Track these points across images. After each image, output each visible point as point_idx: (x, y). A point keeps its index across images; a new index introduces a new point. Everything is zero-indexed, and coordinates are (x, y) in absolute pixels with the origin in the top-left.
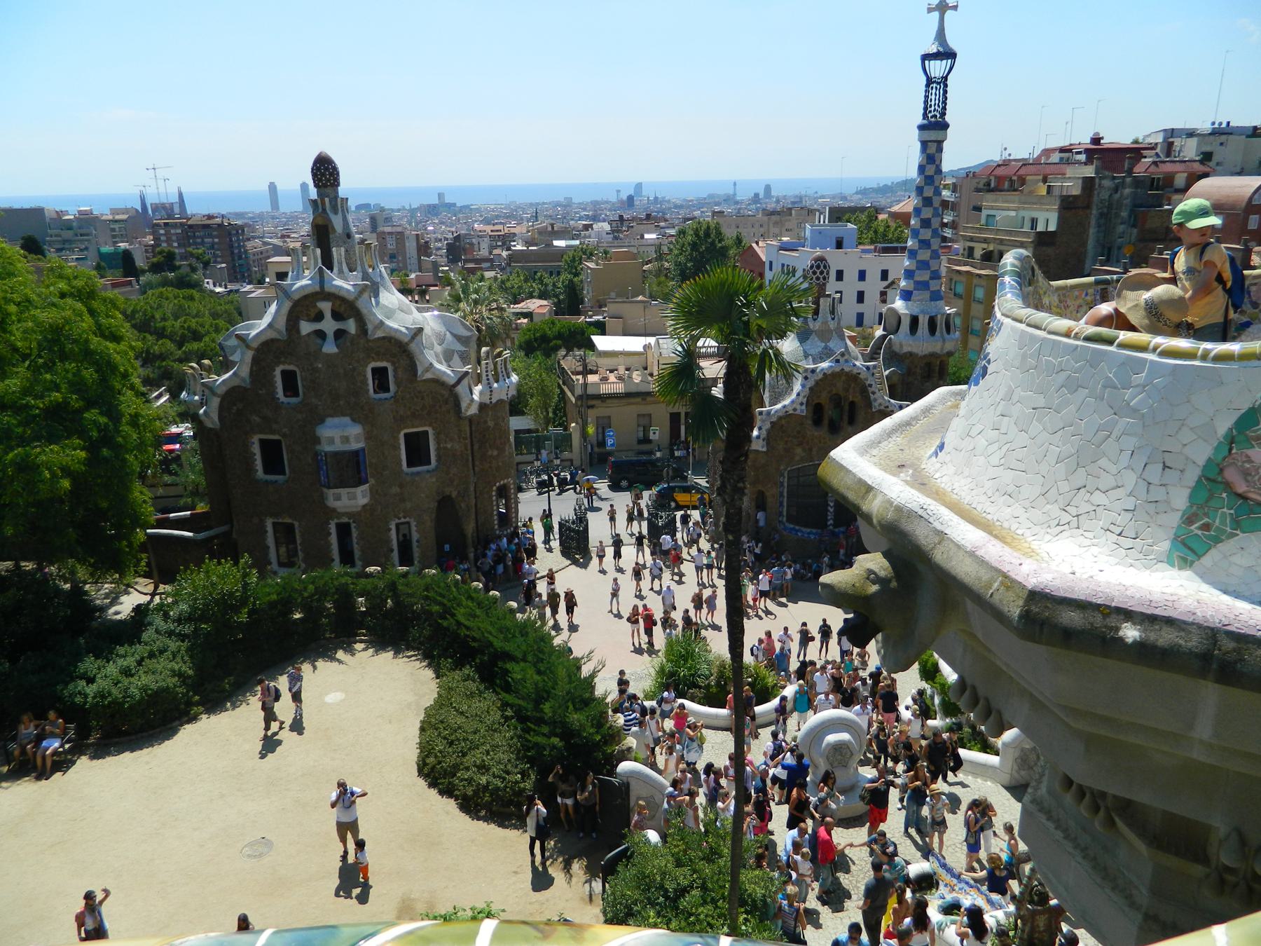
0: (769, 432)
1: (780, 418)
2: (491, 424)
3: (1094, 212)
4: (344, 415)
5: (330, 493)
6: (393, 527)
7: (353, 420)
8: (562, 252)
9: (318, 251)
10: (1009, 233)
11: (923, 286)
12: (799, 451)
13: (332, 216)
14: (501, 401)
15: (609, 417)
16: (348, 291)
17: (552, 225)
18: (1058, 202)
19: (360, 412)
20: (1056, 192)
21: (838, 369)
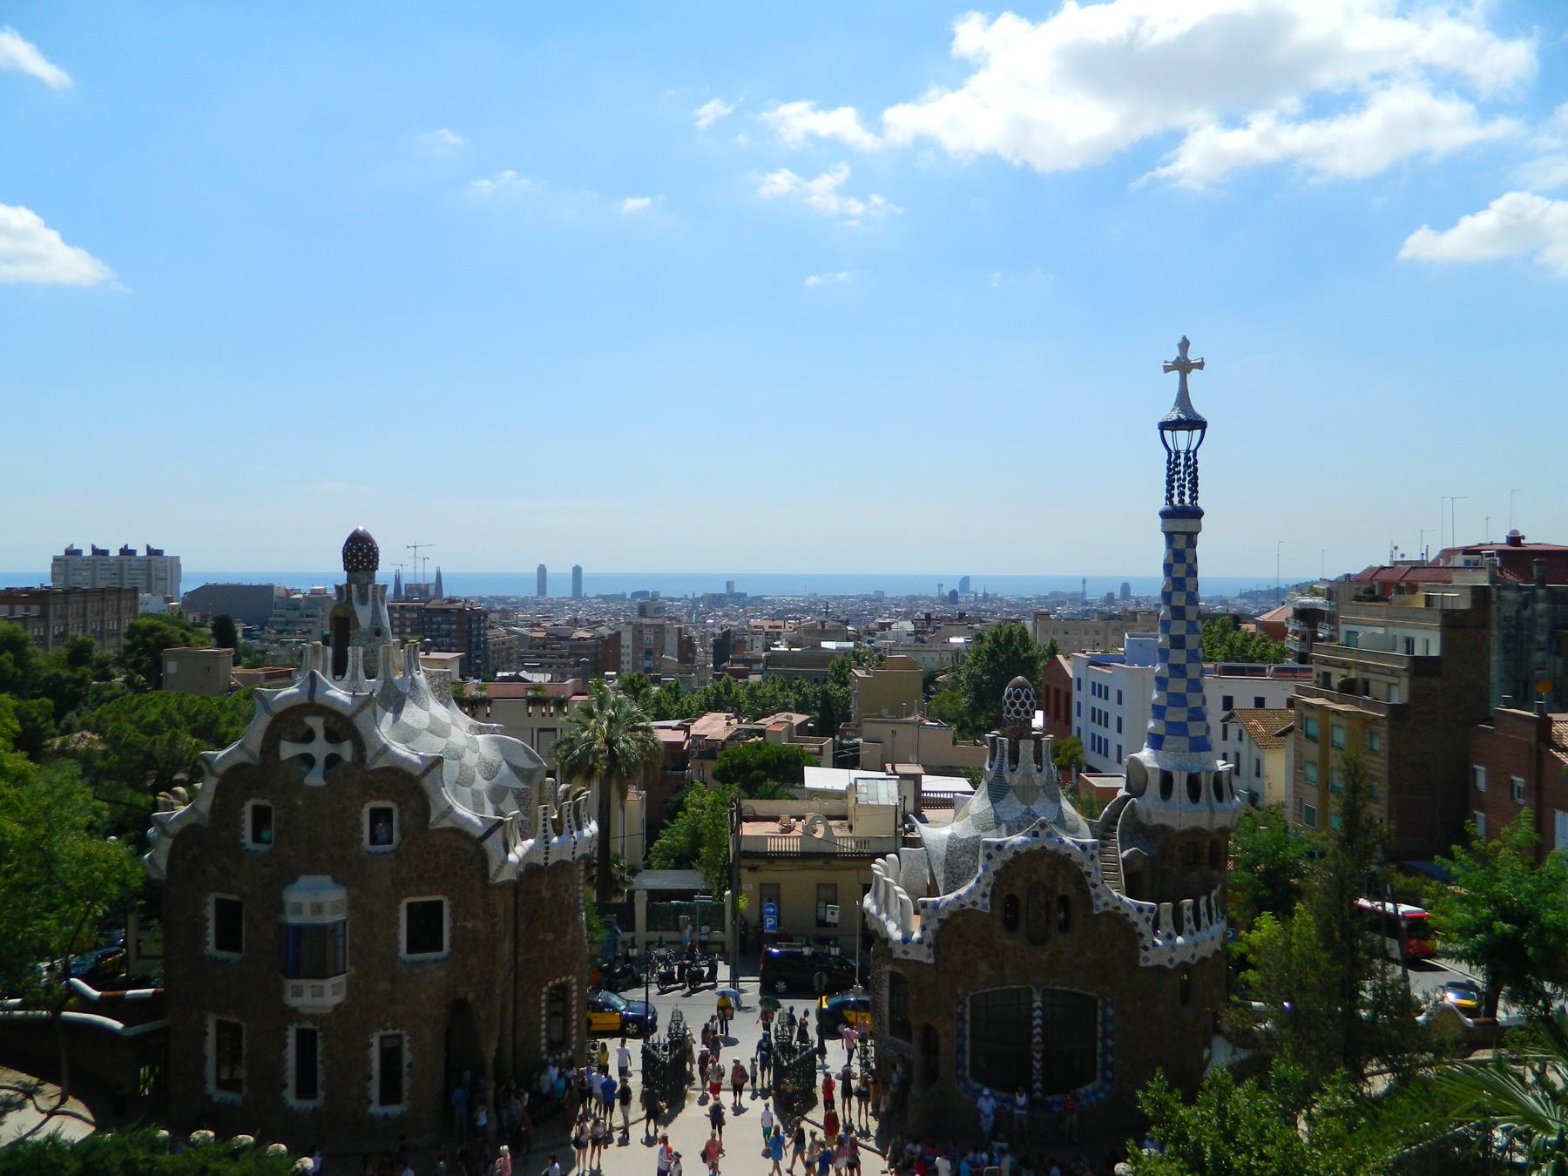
0: (938, 935)
1: (953, 915)
2: (546, 894)
3: (1495, 633)
4: (323, 872)
5: (290, 983)
6: (375, 1041)
7: (336, 881)
8: (831, 654)
9: (330, 650)
10: (1375, 656)
11: (1178, 729)
12: (984, 967)
13: (358, 608)
14: (561, 865)
15: (778, 885)
16: (344, 703)
17: (823, 623)
18: (1439, 617)
19: (347, 870)
20: (1437, 606)
21: (1036, 847)
